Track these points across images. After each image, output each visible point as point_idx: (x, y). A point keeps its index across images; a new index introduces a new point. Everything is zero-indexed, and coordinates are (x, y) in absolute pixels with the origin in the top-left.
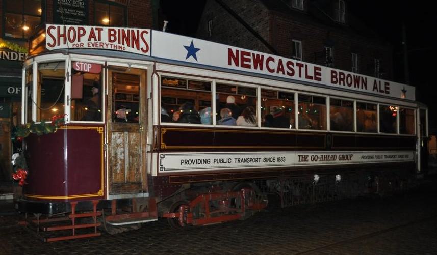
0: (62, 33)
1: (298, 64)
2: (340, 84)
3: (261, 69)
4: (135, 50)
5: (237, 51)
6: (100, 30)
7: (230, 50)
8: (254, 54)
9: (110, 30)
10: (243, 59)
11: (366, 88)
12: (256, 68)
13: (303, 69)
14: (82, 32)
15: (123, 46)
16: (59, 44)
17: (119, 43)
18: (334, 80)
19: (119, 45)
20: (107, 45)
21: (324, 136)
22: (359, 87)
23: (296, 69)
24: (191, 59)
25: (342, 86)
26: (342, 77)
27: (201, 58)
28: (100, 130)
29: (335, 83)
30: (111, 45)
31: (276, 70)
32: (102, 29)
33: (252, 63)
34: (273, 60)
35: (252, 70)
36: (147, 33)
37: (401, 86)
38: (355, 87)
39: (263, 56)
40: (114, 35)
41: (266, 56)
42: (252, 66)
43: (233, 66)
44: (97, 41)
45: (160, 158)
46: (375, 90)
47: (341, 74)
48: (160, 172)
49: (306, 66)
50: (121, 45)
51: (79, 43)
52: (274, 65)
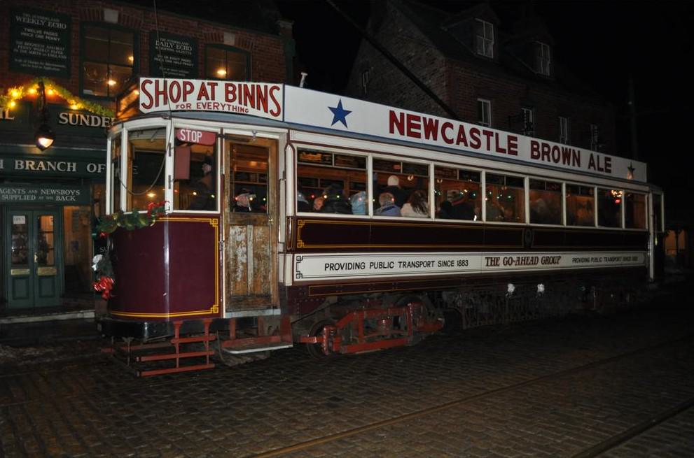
0: (161, 89)
1: (485, 132)
2: (543, 159)
3: (435, 138)
4: (261, 113)
5: (402, 115)
6: (213, 86)
7: (392, 113)
8: (425, 119)
9: (227, 86)
10: (410, 126)
11: (579, 165)
12: (427, 137)
13: (493, 139)
14: (188, 88)
15: (245, 107)
16: (157, 105)
17: (240, 103)
18: (536, 153)
19: (240, 106)
20: (223, 106)
21: (521, 231)
22: (569, 164)
23: (483, 138)
24: (339, 126)
25: (546, 162)
26: (546, 149)
27: (353, 124)
28: (213, 223)
29: (537, 157)
30: (229, 106)
31: (455, 141)
32: (217, 84)
33: (422, 131)
34: (451, 126)
35: (423, 140)
36: (278, 89)
38: (564, 163)
39: (437, 121)
40: (233, 92)
41: (442, 121)
42: (423, 135)
43: (397, 135)
44: (210, 101)
45: (295, 261)
46: (592, 168)
47: (544, 145)
48: (295, 280)
49: (497, 134)
50: (243, 106)
51: (185, 103)
52: (452, 134)
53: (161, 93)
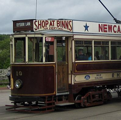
0: (40, 23)
6: (54, 21)
9: (57, 21)
16: (39, 29)
17: (61, 27)
24: (86, 31)
27: (90, 30)
28: (54, 66)
31: (117, 31)
32: (54, 21)
33: (107, 30)
35: (108, 33)
39: (112, 25)
40: (59, 23)
43: (101, 32)
50: (62, 28)
53: (40, 25)
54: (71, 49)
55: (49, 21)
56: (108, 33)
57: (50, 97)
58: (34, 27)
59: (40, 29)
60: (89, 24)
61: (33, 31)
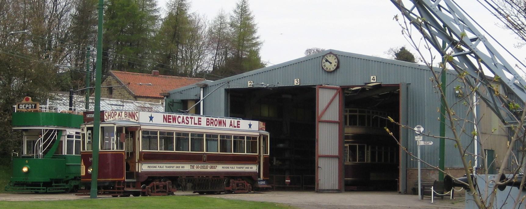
4: (133, 120)
23: (190, 120)
25: (212, 126)
37: (248, 122)
41: (177, 116)
47: (211, 119)
52: (180, 120)
54: (139, 139)
55: (118, 112)
56: (172, 123)
57: (119, 182)
58: (105, 117)
59: (110, 120)
60: (154, 115)
61: (104, 121)
